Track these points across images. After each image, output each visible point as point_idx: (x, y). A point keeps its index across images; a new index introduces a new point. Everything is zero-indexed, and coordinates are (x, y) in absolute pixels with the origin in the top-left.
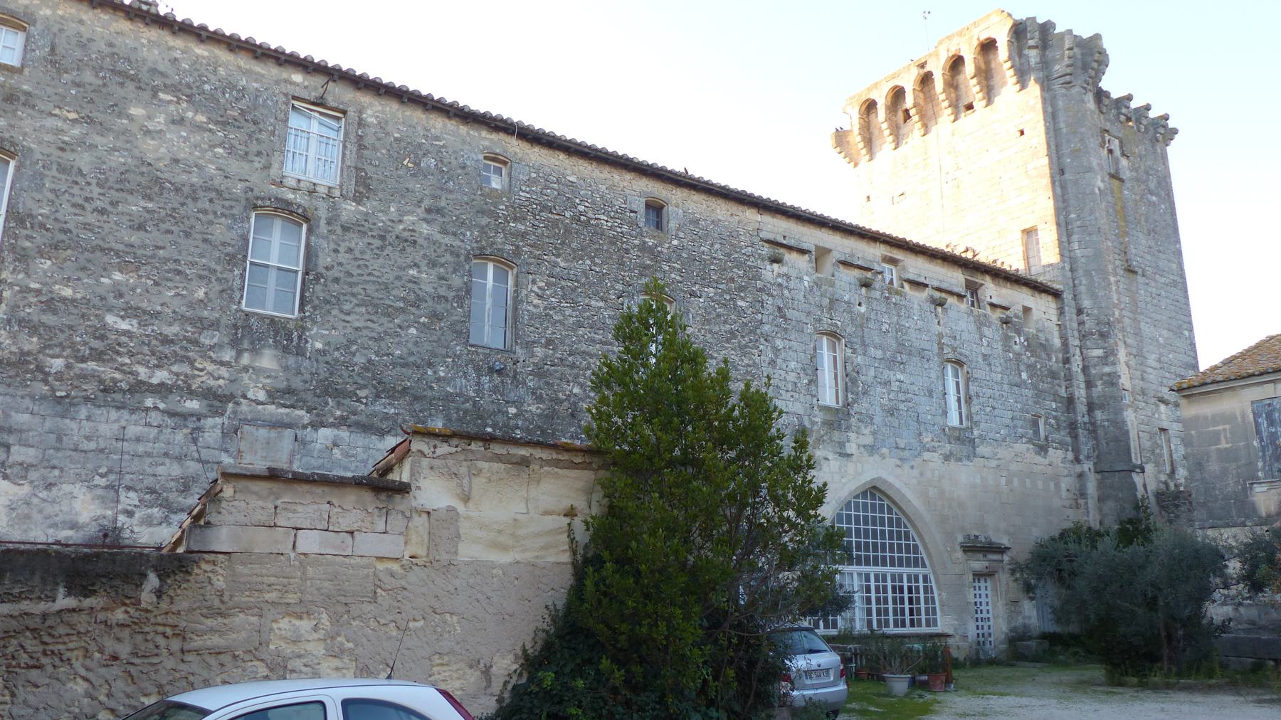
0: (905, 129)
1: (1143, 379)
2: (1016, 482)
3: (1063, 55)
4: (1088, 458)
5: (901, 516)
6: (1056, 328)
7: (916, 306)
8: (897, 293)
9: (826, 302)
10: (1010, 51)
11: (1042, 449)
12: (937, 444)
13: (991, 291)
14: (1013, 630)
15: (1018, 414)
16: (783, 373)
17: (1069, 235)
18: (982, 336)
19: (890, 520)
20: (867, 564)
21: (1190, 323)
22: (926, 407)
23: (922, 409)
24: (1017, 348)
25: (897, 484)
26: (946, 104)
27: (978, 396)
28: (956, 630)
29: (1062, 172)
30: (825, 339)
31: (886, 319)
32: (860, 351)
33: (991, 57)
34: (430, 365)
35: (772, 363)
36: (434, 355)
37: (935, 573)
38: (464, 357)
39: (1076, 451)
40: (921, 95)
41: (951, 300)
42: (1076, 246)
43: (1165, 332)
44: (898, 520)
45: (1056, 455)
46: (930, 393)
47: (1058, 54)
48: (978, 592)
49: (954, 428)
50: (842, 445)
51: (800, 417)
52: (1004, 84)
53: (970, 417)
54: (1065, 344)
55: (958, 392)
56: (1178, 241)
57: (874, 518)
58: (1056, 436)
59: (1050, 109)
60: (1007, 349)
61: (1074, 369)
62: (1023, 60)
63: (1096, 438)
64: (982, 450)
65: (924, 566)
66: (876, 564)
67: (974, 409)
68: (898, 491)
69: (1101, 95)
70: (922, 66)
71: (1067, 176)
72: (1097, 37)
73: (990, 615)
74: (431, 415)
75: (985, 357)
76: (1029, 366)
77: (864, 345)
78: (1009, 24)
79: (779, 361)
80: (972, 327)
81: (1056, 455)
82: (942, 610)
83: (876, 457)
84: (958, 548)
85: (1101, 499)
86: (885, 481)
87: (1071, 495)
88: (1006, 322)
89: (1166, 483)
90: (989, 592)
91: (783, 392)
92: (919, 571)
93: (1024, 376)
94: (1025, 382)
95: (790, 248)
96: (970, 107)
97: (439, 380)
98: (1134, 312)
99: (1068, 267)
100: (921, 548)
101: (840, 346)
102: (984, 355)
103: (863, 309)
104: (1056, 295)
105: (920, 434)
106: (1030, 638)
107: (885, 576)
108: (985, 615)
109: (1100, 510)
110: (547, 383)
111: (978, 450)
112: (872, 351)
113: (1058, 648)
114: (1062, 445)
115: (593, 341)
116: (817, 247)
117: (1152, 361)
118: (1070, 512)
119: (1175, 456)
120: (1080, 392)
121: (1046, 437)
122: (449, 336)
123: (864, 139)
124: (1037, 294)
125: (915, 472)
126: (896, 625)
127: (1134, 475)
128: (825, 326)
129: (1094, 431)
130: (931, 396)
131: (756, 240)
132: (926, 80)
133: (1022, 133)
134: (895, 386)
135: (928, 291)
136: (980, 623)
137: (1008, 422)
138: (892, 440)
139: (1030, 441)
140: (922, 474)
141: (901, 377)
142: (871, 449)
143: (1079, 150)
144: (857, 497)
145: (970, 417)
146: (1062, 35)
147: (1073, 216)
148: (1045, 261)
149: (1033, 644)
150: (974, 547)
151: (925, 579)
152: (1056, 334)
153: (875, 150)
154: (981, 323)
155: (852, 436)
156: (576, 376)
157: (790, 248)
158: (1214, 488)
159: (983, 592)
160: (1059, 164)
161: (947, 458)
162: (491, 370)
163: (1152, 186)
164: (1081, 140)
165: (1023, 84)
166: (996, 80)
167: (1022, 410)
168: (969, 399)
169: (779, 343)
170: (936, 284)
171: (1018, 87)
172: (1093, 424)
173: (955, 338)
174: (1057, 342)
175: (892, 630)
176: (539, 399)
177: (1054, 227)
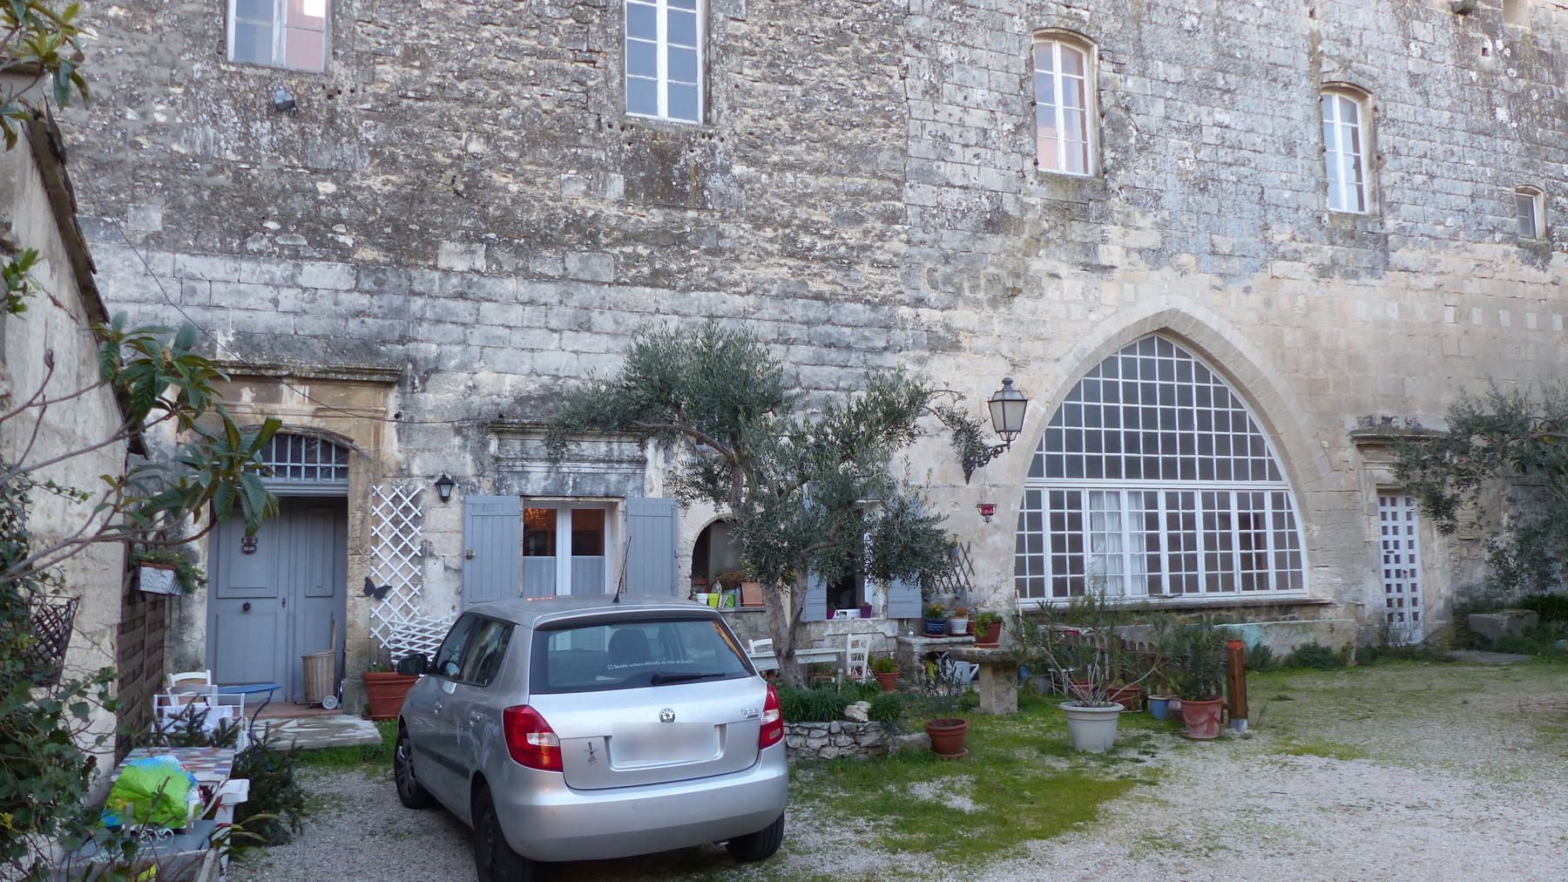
2: (1477, 317)
5: (1225, 383)
15: (1485, 187)
16: (957, 112)
19: (1203, 392)
22: (1281, 177)
23: (1269, 179)
24: (1487, 61)
25: (1214, 323)
27: (1396, 152)
28: (1338, 593)
30: (1057, 48)
32: (1131, 65)
34: (131, 100)
35: (932, 91)
36: (140, 80)
37: (1297, 490)
38: (212, 84)
46: (1290, 149)
49: (1344, 216)
50: (1089, 248)
51: (994, 196)
53: (1378, 194)
64: (1401, 256)
65: (1275, 476)
67: (1386, 180)
68: (1217, 336)
73: (1417, 566)
74: (134, 198)
75: (1414, 79)
76: (1513, 97)
77: (1141, 53)
79: (947, 89)
80: (1387, 21)
82: (1311, 558)
83: (1167, 271)
84: (1346, 441)
86: (1187, 318)
91: (957, 149)
92: (1266, 486)
93: (1502, 114)
94: (1503, 126)
97: (153, 129)
100: (1269, 444)
101: (1090, 61)
105: (1266, 227)
108: (1404, 565)
110: (409, 134)
111: (1394, 257)
112: (1159, 68)
115: (515, 50)
121: (1548, 232)
122: (176, 43)
125: (1254, 299)
126: (1212, 585)
134: (1210, 135)
136: (1394, 581)
137: (1463, 202)
139: (1511, 238)
140: (1268, 303)
141: (1225, 118)
142: (1156, 257)
144: (1130, 349)
145: (1378, 194)
149: (1502, 618)
151: (1278, 500)
155: (1113, 231)
156: (477, 120)
161: (1324, 272)
162: (278, 110)
167: (1495, 180)
169: (947, 53)
173: (1348, 43)
175: (1203, 596)
176: (390, 164)
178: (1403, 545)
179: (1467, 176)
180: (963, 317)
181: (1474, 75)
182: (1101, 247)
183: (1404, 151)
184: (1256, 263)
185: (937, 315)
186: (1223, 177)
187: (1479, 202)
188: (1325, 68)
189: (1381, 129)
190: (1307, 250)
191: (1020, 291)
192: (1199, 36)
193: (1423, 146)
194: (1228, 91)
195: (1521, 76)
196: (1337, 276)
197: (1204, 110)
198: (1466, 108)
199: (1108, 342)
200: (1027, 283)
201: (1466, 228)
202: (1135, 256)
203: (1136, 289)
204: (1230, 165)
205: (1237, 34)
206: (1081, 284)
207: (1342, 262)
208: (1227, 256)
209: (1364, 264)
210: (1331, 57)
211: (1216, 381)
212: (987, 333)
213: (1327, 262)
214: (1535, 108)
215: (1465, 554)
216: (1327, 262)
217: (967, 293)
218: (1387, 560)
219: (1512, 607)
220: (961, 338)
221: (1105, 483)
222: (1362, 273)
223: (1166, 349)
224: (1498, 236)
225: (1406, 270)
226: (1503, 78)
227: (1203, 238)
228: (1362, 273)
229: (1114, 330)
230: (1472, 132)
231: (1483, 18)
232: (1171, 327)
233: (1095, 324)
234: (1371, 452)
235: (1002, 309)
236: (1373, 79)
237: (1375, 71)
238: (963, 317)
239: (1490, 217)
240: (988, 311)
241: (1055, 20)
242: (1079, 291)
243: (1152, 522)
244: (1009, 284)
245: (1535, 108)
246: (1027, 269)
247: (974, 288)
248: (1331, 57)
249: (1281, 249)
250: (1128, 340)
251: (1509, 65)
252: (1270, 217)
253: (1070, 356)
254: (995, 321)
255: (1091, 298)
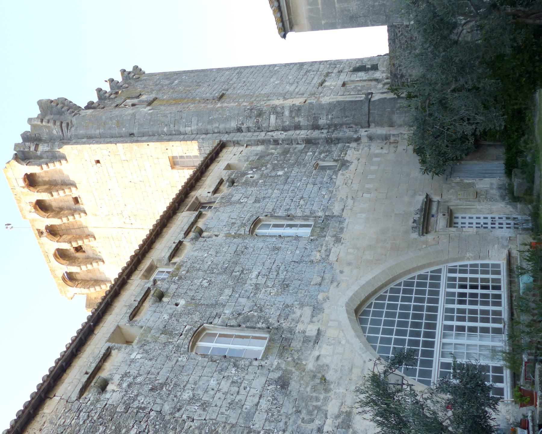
0: (89, 253)
1: (303, 94)
2: (370, 186)
3: (46, 127)
4: (356, 132)
5: (388, 288)
6: (249, 148)
7: (196, 254)
8: (178, 269)
9: (163, 338)
10: (34, 165)
11: (344, 164)
12: (324, 248)
13: (203, 192)
14: (503, 198)
15: (311, 180)
16: (218, 395)
17: (180, 133)
18: (239, 202)
19: (391, 299)
20: (434, 326)
21: (270, 66)
22: (288, 254)
23: (289, 257)
26: (71, 218)
27: (288, 210)
28: (503, 247)
29: (132, 134)
30: (200, 344)
31: (197, 282)
32: (219, 310)
33: (40, 179)
35: (205, 406)
37: (447, 262)
39: (350, 140)
40: (64, 237)
41: (201, 224)
42: (188, 129)
43: (272, 80)
44: (392, 290)
45: (351, 155)
46: (276, 249)
47: (46, 131)
48: (467, 225)
50: (306, 340)
51: (268, 382)
52: (61, 172)
53: (306, 218)
54: (262, 142)
55: (281, 226)
56: (211, 70)
57: (388, 315)
58: (335, 155)
59: (84, 140)
60: (255, 184)
61: (283, 136)
62: (45, 156)
63: (341, 125)
64: (336, 210)
65: (439, 271)
66: (435, 318)
67: (299, 213)
68: (363, 287)
69: (90, 106)
70: (41, 233)
71: (135, 131)
72: (41, 104)
75: (257, 201)
76: (274, 169)
77: (213, 306)
78: (14, 163)
79: (205, 398)
80: (228, 209)
81: (351, 155)
82: (483, 259)
83: (325, 306)
84: (423, 238)
85: (391, 125)
86: (351, 299)
87: (386, 147)
88: (232, 182)
89: (384, 84)
90: (467, 216)
91: (239, 397)
93: (280, 173)
94: (285, 173)
95: (98, 368)
96: (76, 200)
98: (252, 96)
99: (204, 136)
100: (422, 272)
101: (211, 329)
102: (255, 202)
103: (182, 302)
104: (222, 146)
105: (312, 262)
106: (511, 185)
107: (447, 310)
108: (489, 221)
109: (400, 126)
111: (336, 213)
112: (223, 298)
113: (519, 160)
114: (344, 150)
116: (109, 341)
117: (292, 89)
118: (400, 148)
119: (364, 78)
120: (303, 134)
121: (335, 161)
123: (93, 286)
124: (218, 159)
125: (347, 269)
126: (499, 304)
127: (373, 99)
128: (184, 341)
129: (335, 126)
130: (278, 249)
131: (76, 405)
132: (52, 231)
133: (98, 162)
134: (261, 280)
135: (187, 243)
137: (316, 188)
138: (311, 288)
139: (336, 173)
140: (349, 264)
141: (255, 273)
142: (317, 309)
143: (118, 121)
144: (364, 330)
145: (306, 218)
146: (33, 126)
147: (165, 129)
148: (197, 153)
150: (424, 223)
151: (452, 270)
152: (254, 148)
153: (103, 278)
154: (228, 201)
155: (300, 327)
157: (98, 368)
158: (373, 6)
159: (467, 221)
160: (126, 137)
161: (338, 240)
163: (167, 82)
164: (111, 119)
165: (61, 158)
166: (57, 177)
168: (289, 217)
169: (186, 396)
170: (182, 235)
171: (63, 162)
172: (329, 126)
173: (234, 223)
174: (260, 148)
175: (504, 308)
177: (171, 143)
178: (478, 221)
179: (305, 186)
180: (333, 408)
181: (260, 181)
182: (307, 334)
183: (288, 207)
184: (328, 267)
185: (329, 421)
186: (283, 277)
187: (317, 182)
188: (243, 233)
189: (276, 214)
190: (326, 246)
191: (323, 376)
192: (213, 280)
193: (287, 200)
194: (242, 271)
195: (266, 166)
196: (341, 236)
197: (249, 282)
198: (275, 184)
199: (358, 336)
200: (319, 372)
201: (328, 187)
202: (315, 319)
203: (332, 320)
204: (278, 273)
205: (217, 265)
206: (324, 346)
207: (335, 233)
208: (323, 279)
209: (337, 225)
210: (238, 230)
211: (386, 292)
212: (344, 396)
213: (334, 239)
214: (281, 162)
215: (484, 196)
216: (334, 239)
217: (319, 404)
218: (487, 228)
219: (511, 180)
220: (344, 410)
221: (437, 350)
222: (341, 226)
223: (366, 313)
224: (334, 177)
225: (343, 210)
226: (265, 172)
227: (311, 288)
228: (341, 226)
229: (352, 333)
230: (285, 183)
231: (238, 177)
232: (355, 307)
233: (348, 341)
234: (430, 228)
235: (332, 386)
236: (252, 216)
237: (249, 215)
238: (333, 408)
239: (325, 179)
240: (331, 394)
241: (186, 341)
242: (329, 347)
243: (461, 329)
244: (318, 381)
245: (281, 162)
246: (312, 371)
247: (317, 399)
248: (238, 230)
249: (324, 256)
250: (358, 328)
251: (260, 169)
252: (307, 259)
253: (363, 355)
254: (338, 391)
255: (333, 342)
